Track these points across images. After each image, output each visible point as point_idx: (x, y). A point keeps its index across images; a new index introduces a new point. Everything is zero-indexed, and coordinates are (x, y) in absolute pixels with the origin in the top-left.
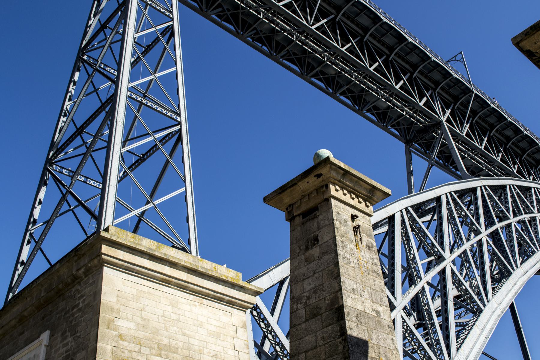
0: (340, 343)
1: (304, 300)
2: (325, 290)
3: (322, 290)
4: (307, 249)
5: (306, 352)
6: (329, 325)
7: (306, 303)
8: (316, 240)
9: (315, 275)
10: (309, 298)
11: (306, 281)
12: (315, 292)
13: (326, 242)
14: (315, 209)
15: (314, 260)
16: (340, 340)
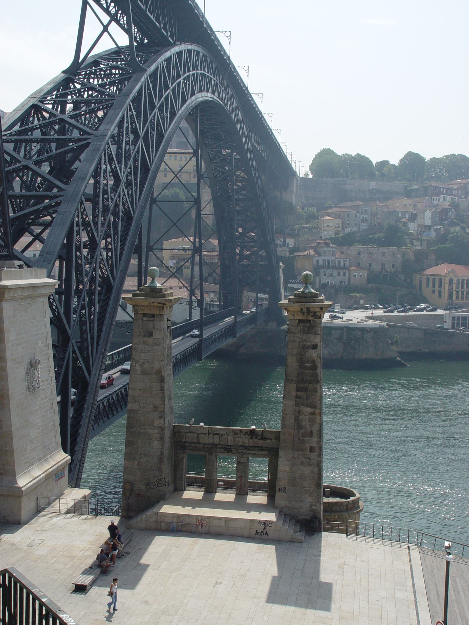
0: (160, 393)
1: (140, 363)
2: (154, 364)
3: (153, 363)
4: (145, 336)
5: (140, 390)
6: (155, 382)
7: (142, 365)
8: (151, 335)
9: (149, 353)
10: (143, 363)
11: (143, 353)
12: (148, 362)
13: (158, 339)
14: (153, 316)
15: (148, 345)
16: (161, 391)
